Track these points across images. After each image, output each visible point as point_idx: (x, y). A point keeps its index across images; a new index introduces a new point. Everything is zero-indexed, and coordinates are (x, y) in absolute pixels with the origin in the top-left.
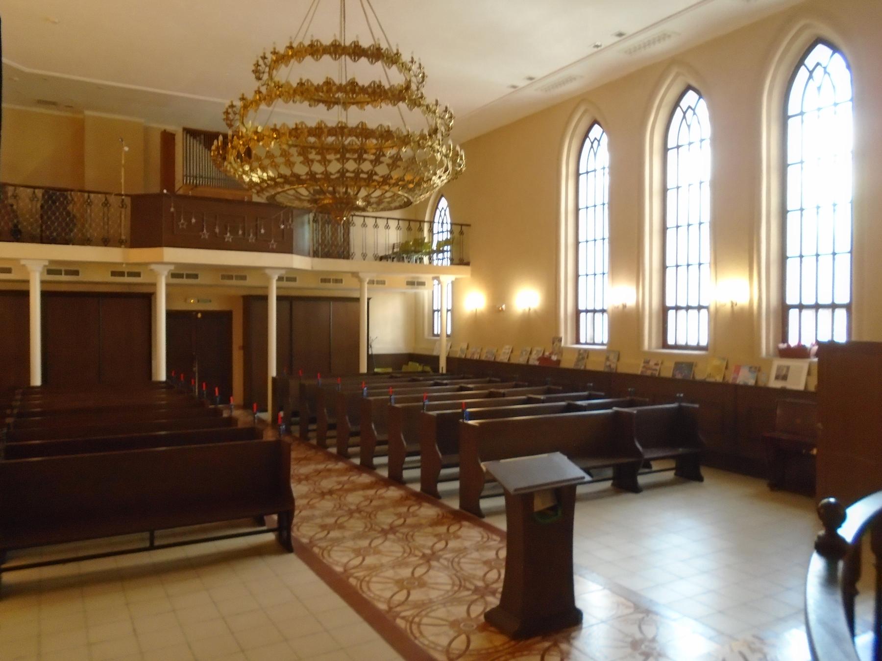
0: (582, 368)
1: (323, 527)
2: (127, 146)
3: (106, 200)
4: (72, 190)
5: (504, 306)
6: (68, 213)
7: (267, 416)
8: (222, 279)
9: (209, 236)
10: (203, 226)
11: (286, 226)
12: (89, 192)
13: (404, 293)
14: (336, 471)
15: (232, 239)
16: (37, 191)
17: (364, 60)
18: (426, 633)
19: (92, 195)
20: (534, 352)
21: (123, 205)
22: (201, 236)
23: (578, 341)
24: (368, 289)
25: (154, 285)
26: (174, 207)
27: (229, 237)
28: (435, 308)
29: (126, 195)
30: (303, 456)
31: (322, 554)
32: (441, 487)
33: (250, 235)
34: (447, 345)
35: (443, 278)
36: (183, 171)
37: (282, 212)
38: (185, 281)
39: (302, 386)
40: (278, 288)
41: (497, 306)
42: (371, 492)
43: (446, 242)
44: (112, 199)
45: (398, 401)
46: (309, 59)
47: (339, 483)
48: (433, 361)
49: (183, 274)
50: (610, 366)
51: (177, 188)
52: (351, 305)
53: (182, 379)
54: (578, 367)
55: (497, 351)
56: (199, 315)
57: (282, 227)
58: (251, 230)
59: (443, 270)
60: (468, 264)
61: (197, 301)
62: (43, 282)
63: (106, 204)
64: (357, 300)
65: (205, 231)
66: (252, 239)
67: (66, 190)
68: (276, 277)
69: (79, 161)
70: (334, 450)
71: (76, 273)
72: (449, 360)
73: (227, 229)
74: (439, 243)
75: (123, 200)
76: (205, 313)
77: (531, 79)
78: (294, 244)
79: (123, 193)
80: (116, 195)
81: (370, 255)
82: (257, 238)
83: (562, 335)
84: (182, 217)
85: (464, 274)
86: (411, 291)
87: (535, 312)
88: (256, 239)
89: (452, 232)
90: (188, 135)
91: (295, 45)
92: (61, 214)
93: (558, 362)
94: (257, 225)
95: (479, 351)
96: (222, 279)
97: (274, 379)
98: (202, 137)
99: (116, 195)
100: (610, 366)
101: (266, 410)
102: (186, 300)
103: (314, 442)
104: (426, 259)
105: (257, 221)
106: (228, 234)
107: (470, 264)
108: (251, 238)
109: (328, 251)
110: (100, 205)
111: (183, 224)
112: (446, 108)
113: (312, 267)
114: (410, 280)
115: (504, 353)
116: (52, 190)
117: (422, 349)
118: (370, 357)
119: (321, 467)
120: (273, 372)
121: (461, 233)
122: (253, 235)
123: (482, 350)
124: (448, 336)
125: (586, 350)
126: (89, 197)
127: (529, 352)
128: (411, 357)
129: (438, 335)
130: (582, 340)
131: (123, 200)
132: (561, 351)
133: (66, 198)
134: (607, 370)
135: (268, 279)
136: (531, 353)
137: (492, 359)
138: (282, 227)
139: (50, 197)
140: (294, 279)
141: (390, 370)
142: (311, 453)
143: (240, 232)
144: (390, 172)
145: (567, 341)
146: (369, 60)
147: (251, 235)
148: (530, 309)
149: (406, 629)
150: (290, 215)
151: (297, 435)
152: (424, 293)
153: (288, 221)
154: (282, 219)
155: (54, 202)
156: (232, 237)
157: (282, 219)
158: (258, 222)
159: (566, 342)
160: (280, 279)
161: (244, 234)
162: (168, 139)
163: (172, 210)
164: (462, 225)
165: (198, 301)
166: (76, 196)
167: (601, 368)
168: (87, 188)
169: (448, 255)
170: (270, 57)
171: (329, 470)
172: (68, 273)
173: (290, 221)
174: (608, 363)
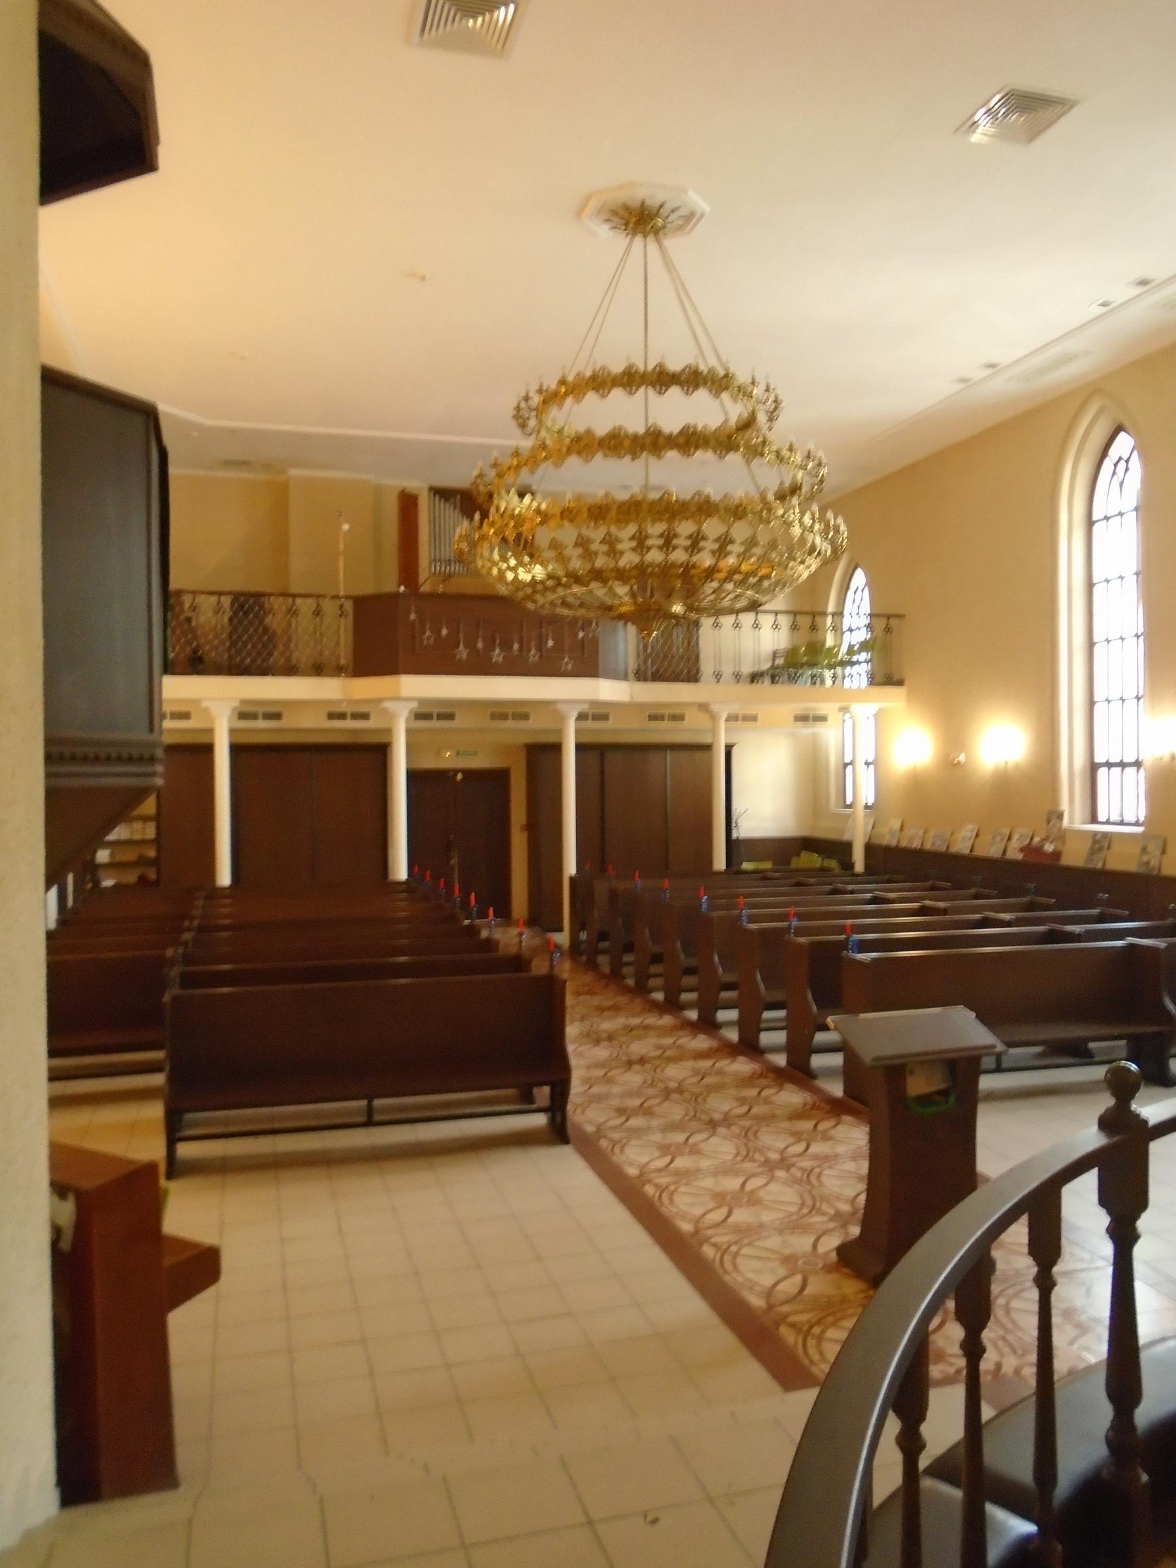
0: (1099, 866)
1: (621, 1111)
2: (346, 521)
4: (270, 595)
5: (962, 758)
6: (266, 630)
7: (562, 938)
9: (468, 655)
12: (294, 596)
14: (660, 1028)
16: (223, 598)
17: (675, 391)
18: (741, 1267)
19: (299, 601)
20: (1016, 837)
23: (1094, 819)
24: (727, 730)
25: (389, 731)
26: (416, 612)
28: (847, 760)
29: (347, 597)
30: (610, 1003)
31: (612, 1149)
32: (818, 1061)
33: (529, 651)
34: (866, 824)
35: (855, 707)
36: (430, 553)
38: (435, 724)
39: (613, 894)
40: (577, 731)
41: (951, 756)
42: (706, 1064)
43: (865, 646)
44: (328, 606)
45: (752, 919)
46: (591, 397)
47: (658, 1047)
48: (839, 850)
50: (1148, 863)
51: (422, 579)
52: (698, 755)
53: (428, 878)
54: (1091, 866)
55: (952, 834)
56: (459, 776)
58: (533, 643)
59: (857, 695)
60: (900, 683)
62: (232, 731)
63: (318, 613)
64: (708, 748)
65: (461, 647)
67: (263, 595)
68: (574, 715)
69: (282, 548)
70: (659, 996)
71: (277, 716)
72: (870, 849)
73: (495, 642)
74: (851, 647)
75: (341, 606)
76: (468, 773)
77: (992, 366)
78: (601, 663)
79: (342, 593)
81: (728, 671)
83: (1065, 806)
84: (428, 626)
85: (893, 700)
86: (806, 731)
87: (1017, 767)
88: (540, 657)
89: (869, 627)
90: (437, 497)
91: (570, 378)
93: (1057, 855)
95: (921, 833)
97: (572, 879)
98: (458, 497)
100: (1148, 863)
101: (560, 929)
102: (438, 753)
103: (631, 982)
104: (828, 674)
105: (541, 627)
106: (497, 651)
107: (906, 682)
109: (657, 671)
112: (809, 453)
113: (632, 697)
114: (799, 712)
115: (964, 838)
117: (825, 830)
118: (732, 845)
119: (636, 1021)
120: (570, 867)
121: (888, 630)
123: (925, 832)
124: (867, 807)
125: (1105, 835)
127: (1007, 838)
128: (808, 844)
129: (850, 806)
130: (1102, 817)
131: (341, 606)
132: (1062, 836)
133: (262, 607)
134: (1142, 870)
135: (562, 719)
136: (1009, 838)
137: (944, 849)
138: (581, 635)
139: (241, 607)
140: (605, 717)
141: (768, 865)
142: (622, 1000)
143: (516, 646)
144: (717, 562)
145: (1073, 818)
146: (683, 389)
147: (533, 652)
148: (1006, 763)
149: (714, 1260)
151: (606, 969)
152: (830, 735)
155: (246, 614)
156: (504, 654)
158: (544, 630)
159: (1071, 821)
160: (581, 717)
161: (521, 649)
162: (408, 503)
163: (413, 616)
164: (889, 617)
165: (458, 754)
166: (276, 603)
167: (1131, 866)
168: (293, 589)
169: (864, 668)
170: (536, 400)
171: (647, 1028)
172: (269, 716)
174: (1145, 859)
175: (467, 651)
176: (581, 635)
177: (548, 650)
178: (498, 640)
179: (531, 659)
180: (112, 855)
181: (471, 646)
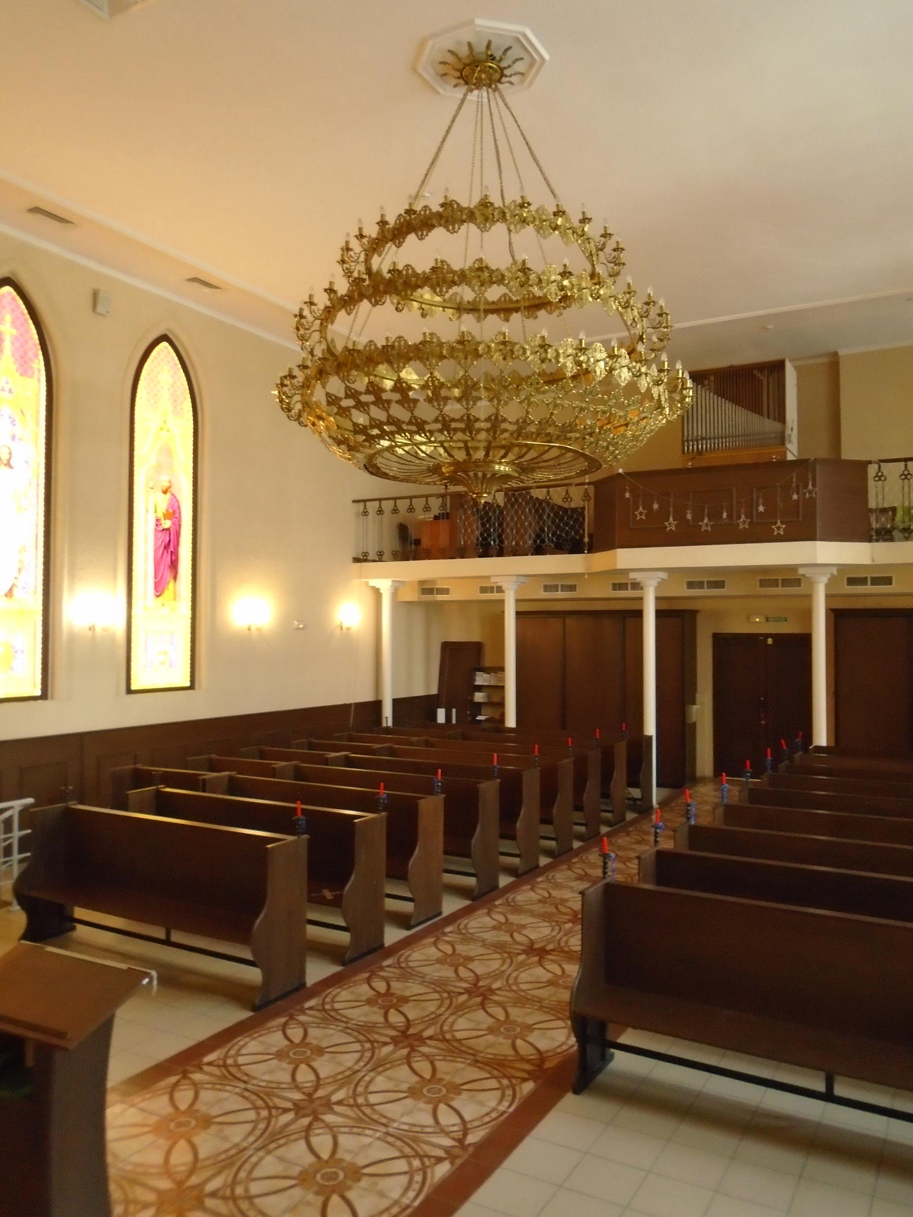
3: (567, 493)
8: (761, 586)
10: (669, 511)
19: (551, 490)
21: (586, 496)
22: (666, 527)
25: (640, 599)
27: (707, 525)
29: (589, 484)
33: (739, 518)
38: (705, 592)
56: (770, 641)
57: (795, 497)
61: (764, 620)
65: (671, 519)
66: (744, 522)
71: (572, 588)
73: (704, 511)
76: (774, 636)
82: (752, 519)
84: (640, 502)
88: (751, 524)
92: (519, 518)
96: (761, 586)
98: (712, 378)
102: (748, 618)
106: (706, 521)
108: (743, 523)
111: (641, 514)
113: (873, 560)
122: (746, 518)
126: (548, 492)
135: (811, 583)
139: (509, 500)
140: (888, 581)
143: (725, 515)
147: (743, 517)
150: (810, 476)
153: (806, 486)
154: (794, 485)
157: (794, 485)
158: (755, 496)
161: (730, 516)
163: (627, 495)
165: (767, 620)
173: (810, 487)
176: (795, 497)
178: (706, 510)
179: (741, 527)
180: (489, 696)
181: (680, 517)
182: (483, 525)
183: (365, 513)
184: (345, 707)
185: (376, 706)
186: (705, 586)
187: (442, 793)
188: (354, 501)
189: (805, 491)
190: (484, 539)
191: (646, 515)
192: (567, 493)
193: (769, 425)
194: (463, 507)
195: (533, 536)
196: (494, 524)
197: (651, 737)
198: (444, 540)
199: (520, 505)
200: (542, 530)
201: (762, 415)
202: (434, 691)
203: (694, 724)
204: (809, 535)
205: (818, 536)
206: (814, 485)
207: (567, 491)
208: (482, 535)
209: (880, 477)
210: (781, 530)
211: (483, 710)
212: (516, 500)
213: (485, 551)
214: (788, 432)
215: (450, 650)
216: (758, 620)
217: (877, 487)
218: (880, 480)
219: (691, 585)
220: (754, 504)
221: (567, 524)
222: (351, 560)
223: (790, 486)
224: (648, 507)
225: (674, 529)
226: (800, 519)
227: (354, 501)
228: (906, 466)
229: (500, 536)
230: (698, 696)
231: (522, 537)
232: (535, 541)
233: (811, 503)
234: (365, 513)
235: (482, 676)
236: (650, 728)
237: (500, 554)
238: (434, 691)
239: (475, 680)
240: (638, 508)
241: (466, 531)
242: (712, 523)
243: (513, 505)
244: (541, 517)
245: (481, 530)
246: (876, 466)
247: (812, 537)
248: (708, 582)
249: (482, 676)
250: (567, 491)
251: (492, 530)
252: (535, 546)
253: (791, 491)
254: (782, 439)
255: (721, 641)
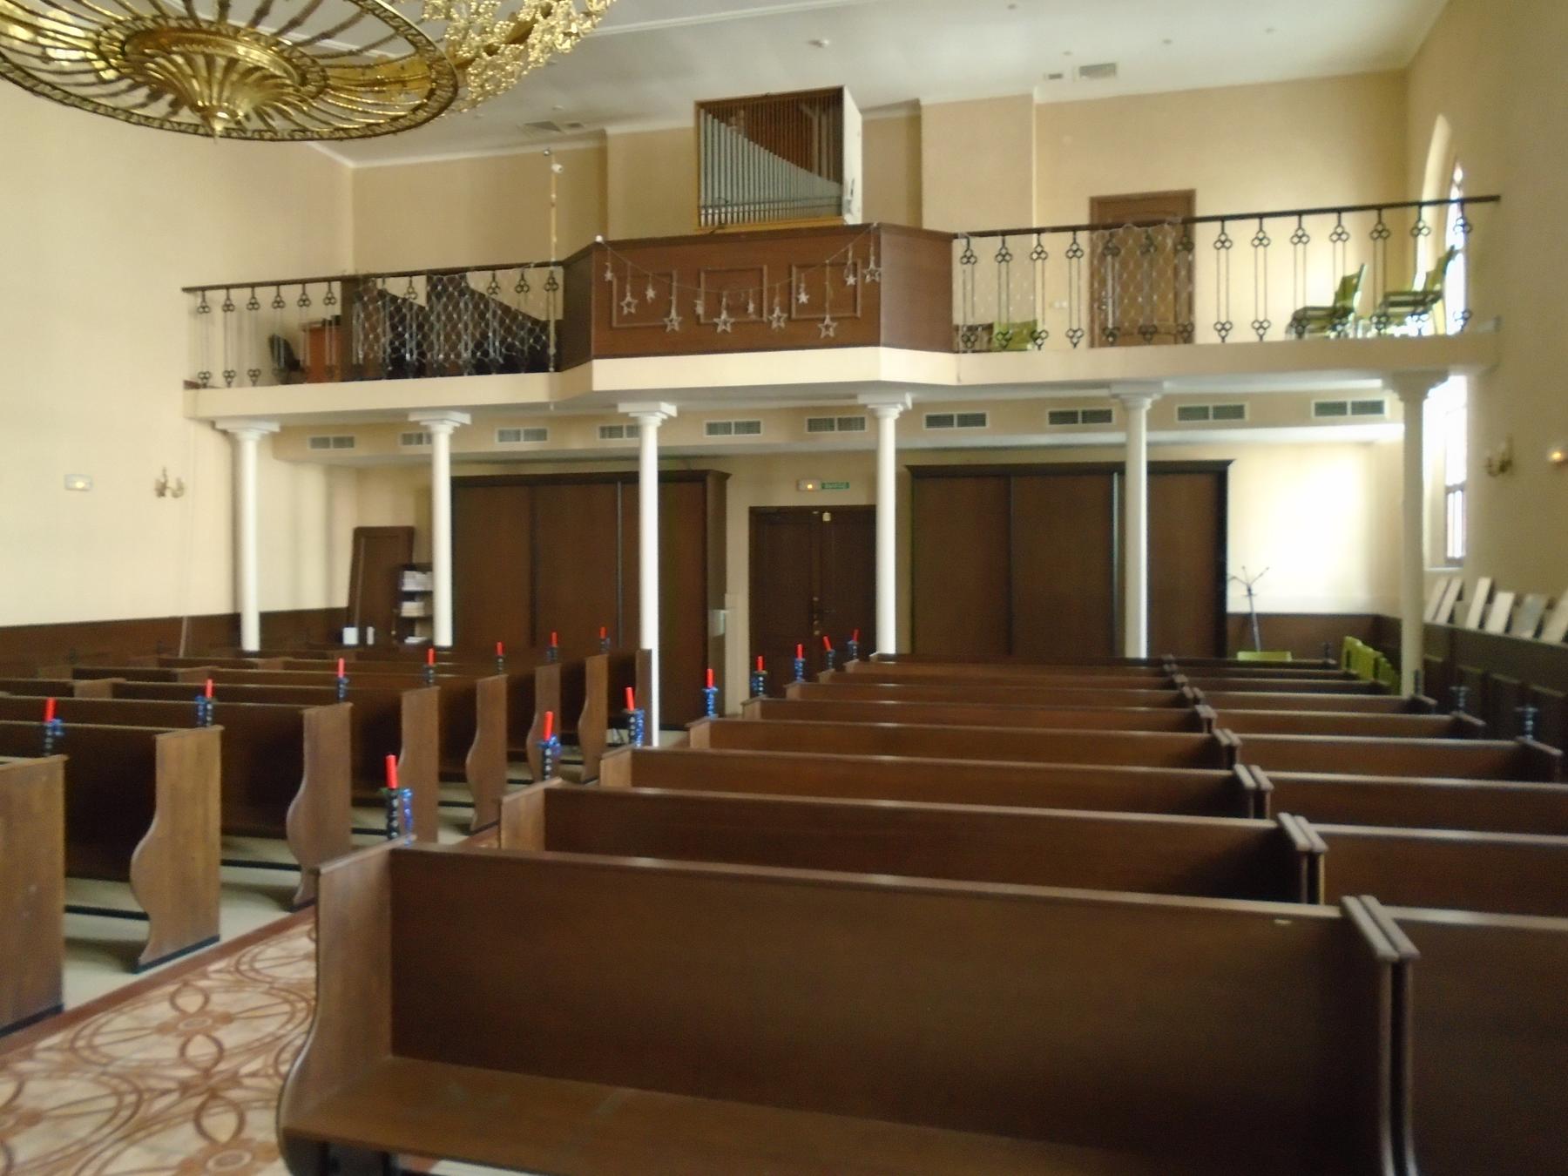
3: (523, 278)
9: (680, 323)
10: (671, 301)
11: (864, 277)
13: (1367, 445)
15: (733, 324)
16: (415, 279)
19: (499, 273)
21: (551, 284)
22: (666, 327)
26: (612, 272)
27: (725, 323)
29: (557, 264)
33: (771, 311)
37: (850, 246)
49: (730, 424)
56: (827, 517)
61: (820, 487)
66: (779, 318)
73: (720, 302)
75: (552, 272)
76: (834, 510)
80: (538, 265)
84: (628, 287)
88: (789, 318)
90: (710, 117)
92: (449, 318)
94: (790, 285)
99: (538, 265)
102: (798, 485)
106: (724, 316)
110: (512, 290)
111: (629, 305)
113: (959, 380)
116: (435, 274)
122: (782, 310)
126: (494, 277)
131: (552, 272)
138: (851, 280)
139: (434, 287)
147: (777, 312)
150: (872, 249)
153: (866, 263)
154: (850, 262)
157: (850, 262)
161: (759, 311)
163: (609, 275)
165: (823, 488)
173: (872, 266)
175: (680, 318)
176: (851, 280)
177: (801, 307)
179: (775, 325)
181: (687, 310)
182: (394, 328)
183: (204, 308)
184: (174, 623)
185: (233, 622)
186: (733, 430)
187: (214, 722)
188: (187, 290)
189: (865, 271)
190: (395, 350)
191: (636, 307)
192: (523, 278)
193: (820, 186)
194: (361, 298)
195: (471, 346)
196: (411, 327)
197: (649, 652)
198: (331, 357)
199: (450, 297)
200: (485, 336)
201: (811, 171)
202: (341, 601)
203: (721, 640)
204: (870, 338)
205: (883, 339)
206: (878, 264)
207: (522, 276)
208: (392, 343)
209: (969, 258)
210: (831, 329)
211: (417, 629)
212: (445, 289)
213: (398, 369)
214: (847, 197)
215: (367, 541)
216: (810, 487)
217: (964, 271)
218: (968, 262)
219: (713, 429)
220: (794, 291)
221: (522, 327)
222: (181, 385)
223: (845, 264)
224: (640, 294)
225: (677, 328)
226: (859, 314)
227: (187, 290)
228: (1004, 242)
229: (419, 345)
230: (728, 598)
231: (454, 347)
232: (474, 354)
233: (876, 285)
234: (204, 308)
235: (414, 577)
236: (650, 638)
237: (421, 370)
238: (341, 601)
239: (403, 584)
240: (625, 296)
241: (366, 337)
242: (733, 320)
243: (439, 297)
244: (482, 315)
245: (390, 336)
246: (964, 241)
247: (874, 341)
248: (737, 425)
249: (414, 577)
250: (522, 276)
251: (407, 336)
252: (473, 362)
253: (846, 271)
254: (839, 207)
255: (761, 519)
